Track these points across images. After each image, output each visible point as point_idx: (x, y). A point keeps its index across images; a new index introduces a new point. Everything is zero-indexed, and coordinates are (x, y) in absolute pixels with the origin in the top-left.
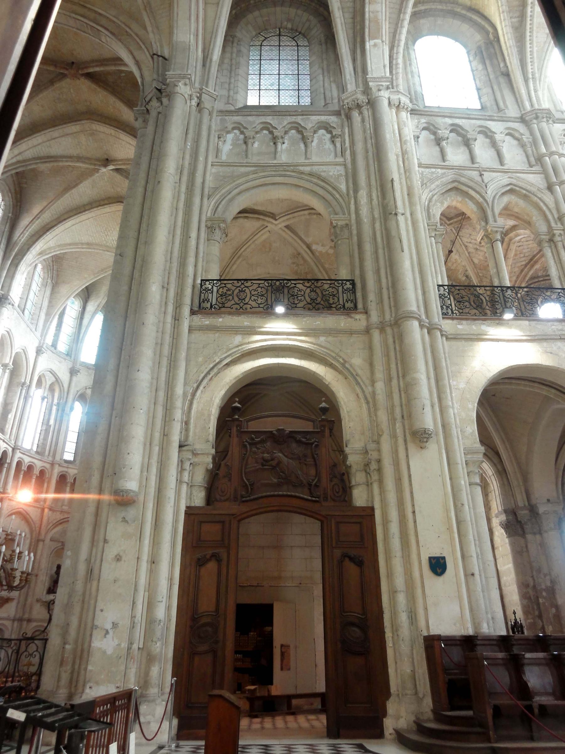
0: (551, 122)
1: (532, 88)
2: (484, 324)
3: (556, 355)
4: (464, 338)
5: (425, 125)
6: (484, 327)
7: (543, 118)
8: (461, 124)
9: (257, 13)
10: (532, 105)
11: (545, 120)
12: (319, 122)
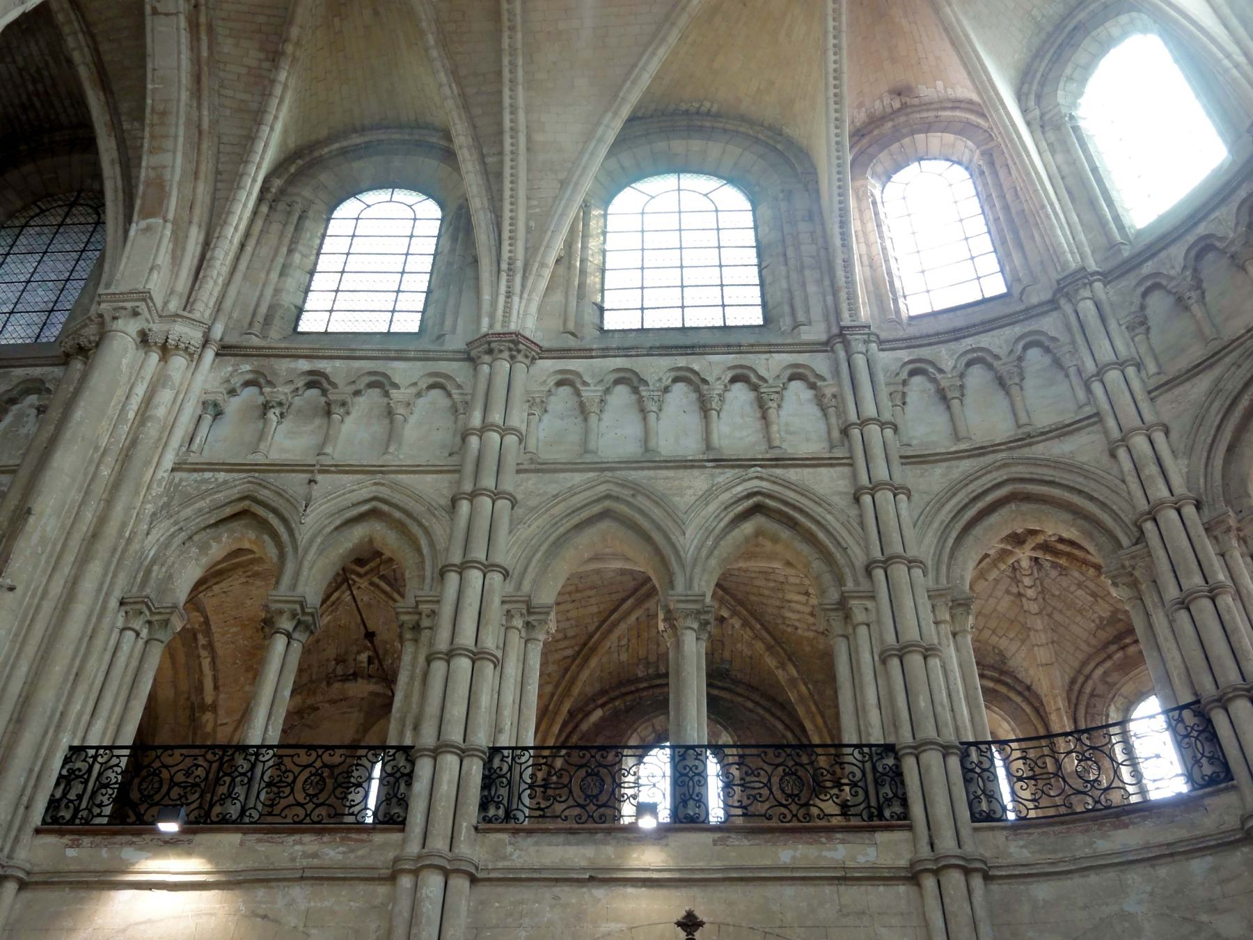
0: (520, 357)
1: (503, 288)
2: (133, 843)
3: (276, 921)
4: (71, 883)
5: (249, 377)
6: (127, 853)
7: (501, 351)
8: (328, 371)
9: (28, 168)
10: (491, 326)
11: (506, 354)
12: (23, 382)
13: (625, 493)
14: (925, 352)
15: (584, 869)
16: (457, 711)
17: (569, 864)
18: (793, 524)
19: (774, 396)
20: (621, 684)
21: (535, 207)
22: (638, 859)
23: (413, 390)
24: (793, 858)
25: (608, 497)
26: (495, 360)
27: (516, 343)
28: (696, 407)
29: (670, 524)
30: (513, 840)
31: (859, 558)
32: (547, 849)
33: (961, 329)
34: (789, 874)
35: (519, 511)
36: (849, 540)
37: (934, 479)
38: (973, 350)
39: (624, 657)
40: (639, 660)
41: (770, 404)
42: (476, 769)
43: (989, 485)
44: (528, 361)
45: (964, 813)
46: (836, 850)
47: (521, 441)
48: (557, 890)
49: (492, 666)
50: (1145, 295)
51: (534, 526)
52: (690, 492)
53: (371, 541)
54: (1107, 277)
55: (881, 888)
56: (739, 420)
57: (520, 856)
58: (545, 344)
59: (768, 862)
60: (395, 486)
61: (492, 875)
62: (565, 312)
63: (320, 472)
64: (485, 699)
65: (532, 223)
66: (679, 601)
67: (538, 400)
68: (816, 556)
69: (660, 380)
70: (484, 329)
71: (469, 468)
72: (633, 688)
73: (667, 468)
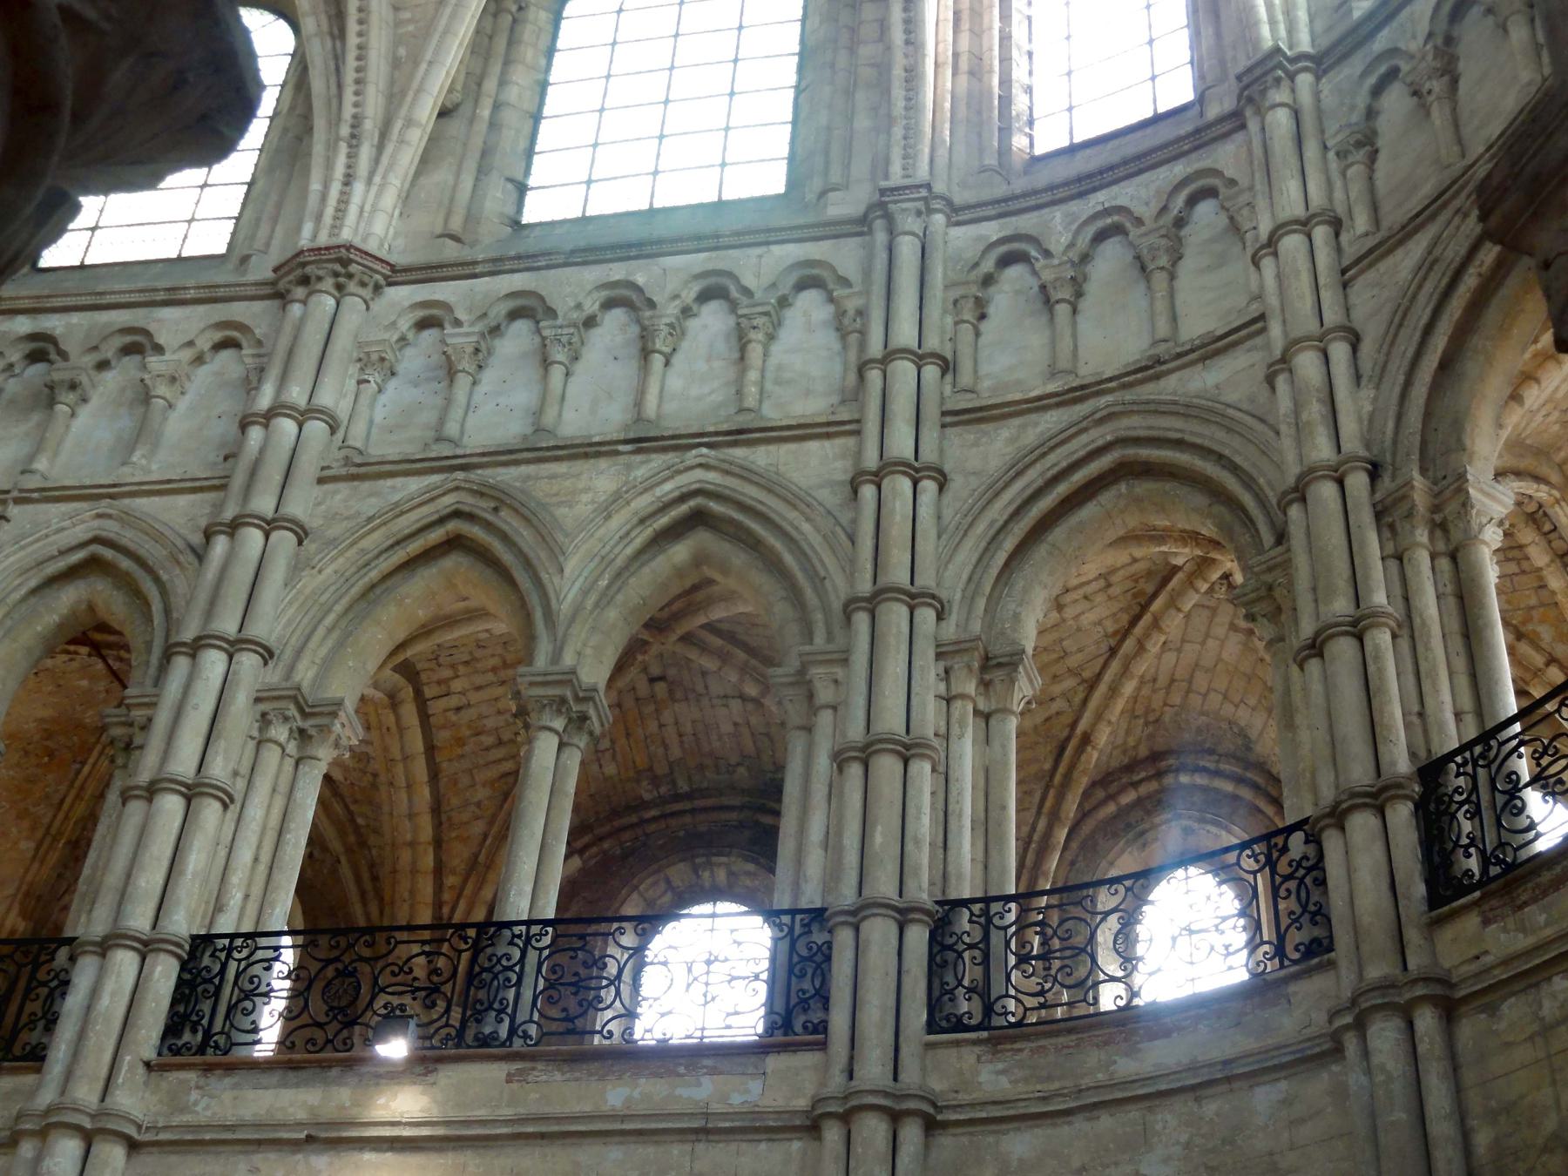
0: (352, 287)
7: (320, 279)
8: (57, 332)
10: (315, 236)
11: (328, 284)
13: (482, 507)
14: (1025, 223)
15: (300, 1125)
16: (150, 879)
17: (280, 1116)
18: (753, 544)
19: (759, 321)
20: (615, 813)
21: (409, 21)
22: (386, 1107)
23: (187, 354)
25: (457, 514)
26: (310, 294)
27: (345, 263)
28: (635, 350)
29: (543, 555)
30: (202, 1082)
32: (251, 1094)
33: (1090, 176)
34: (618, 1126)
35: (310, 546)
36: (830, 564)
37: (995, 448)
38: (1107, 212)
39: (610, 769)
40: (639, 772)
41: (753, 335)
42: (165, 974)
43: (1082, 453)
44: (367, 293)
45: (916, 1016)
46: (699, 1085)
48: (258, 1159)
49: (217, 805)
50: (1377, 91)
51: (329, 570)
52: (585, 498)
53: (91, 608)
54: (1321, 63)
55: (763, 1146)
56: (702, 366)
57: (207, 1108)
58: (393, 259)
59: (587, 1107)
60: (126, 519)
61: (163, 1136)
62: (452, 200)
63: (17, 501)
64: (195, 860)
65: (402, 51)
66: (532, 684)
67: (375, 357)
68: (783, 593)
69: (579, 306)
70: (305, 241)
71: (238, 481)
72: (634, 819)
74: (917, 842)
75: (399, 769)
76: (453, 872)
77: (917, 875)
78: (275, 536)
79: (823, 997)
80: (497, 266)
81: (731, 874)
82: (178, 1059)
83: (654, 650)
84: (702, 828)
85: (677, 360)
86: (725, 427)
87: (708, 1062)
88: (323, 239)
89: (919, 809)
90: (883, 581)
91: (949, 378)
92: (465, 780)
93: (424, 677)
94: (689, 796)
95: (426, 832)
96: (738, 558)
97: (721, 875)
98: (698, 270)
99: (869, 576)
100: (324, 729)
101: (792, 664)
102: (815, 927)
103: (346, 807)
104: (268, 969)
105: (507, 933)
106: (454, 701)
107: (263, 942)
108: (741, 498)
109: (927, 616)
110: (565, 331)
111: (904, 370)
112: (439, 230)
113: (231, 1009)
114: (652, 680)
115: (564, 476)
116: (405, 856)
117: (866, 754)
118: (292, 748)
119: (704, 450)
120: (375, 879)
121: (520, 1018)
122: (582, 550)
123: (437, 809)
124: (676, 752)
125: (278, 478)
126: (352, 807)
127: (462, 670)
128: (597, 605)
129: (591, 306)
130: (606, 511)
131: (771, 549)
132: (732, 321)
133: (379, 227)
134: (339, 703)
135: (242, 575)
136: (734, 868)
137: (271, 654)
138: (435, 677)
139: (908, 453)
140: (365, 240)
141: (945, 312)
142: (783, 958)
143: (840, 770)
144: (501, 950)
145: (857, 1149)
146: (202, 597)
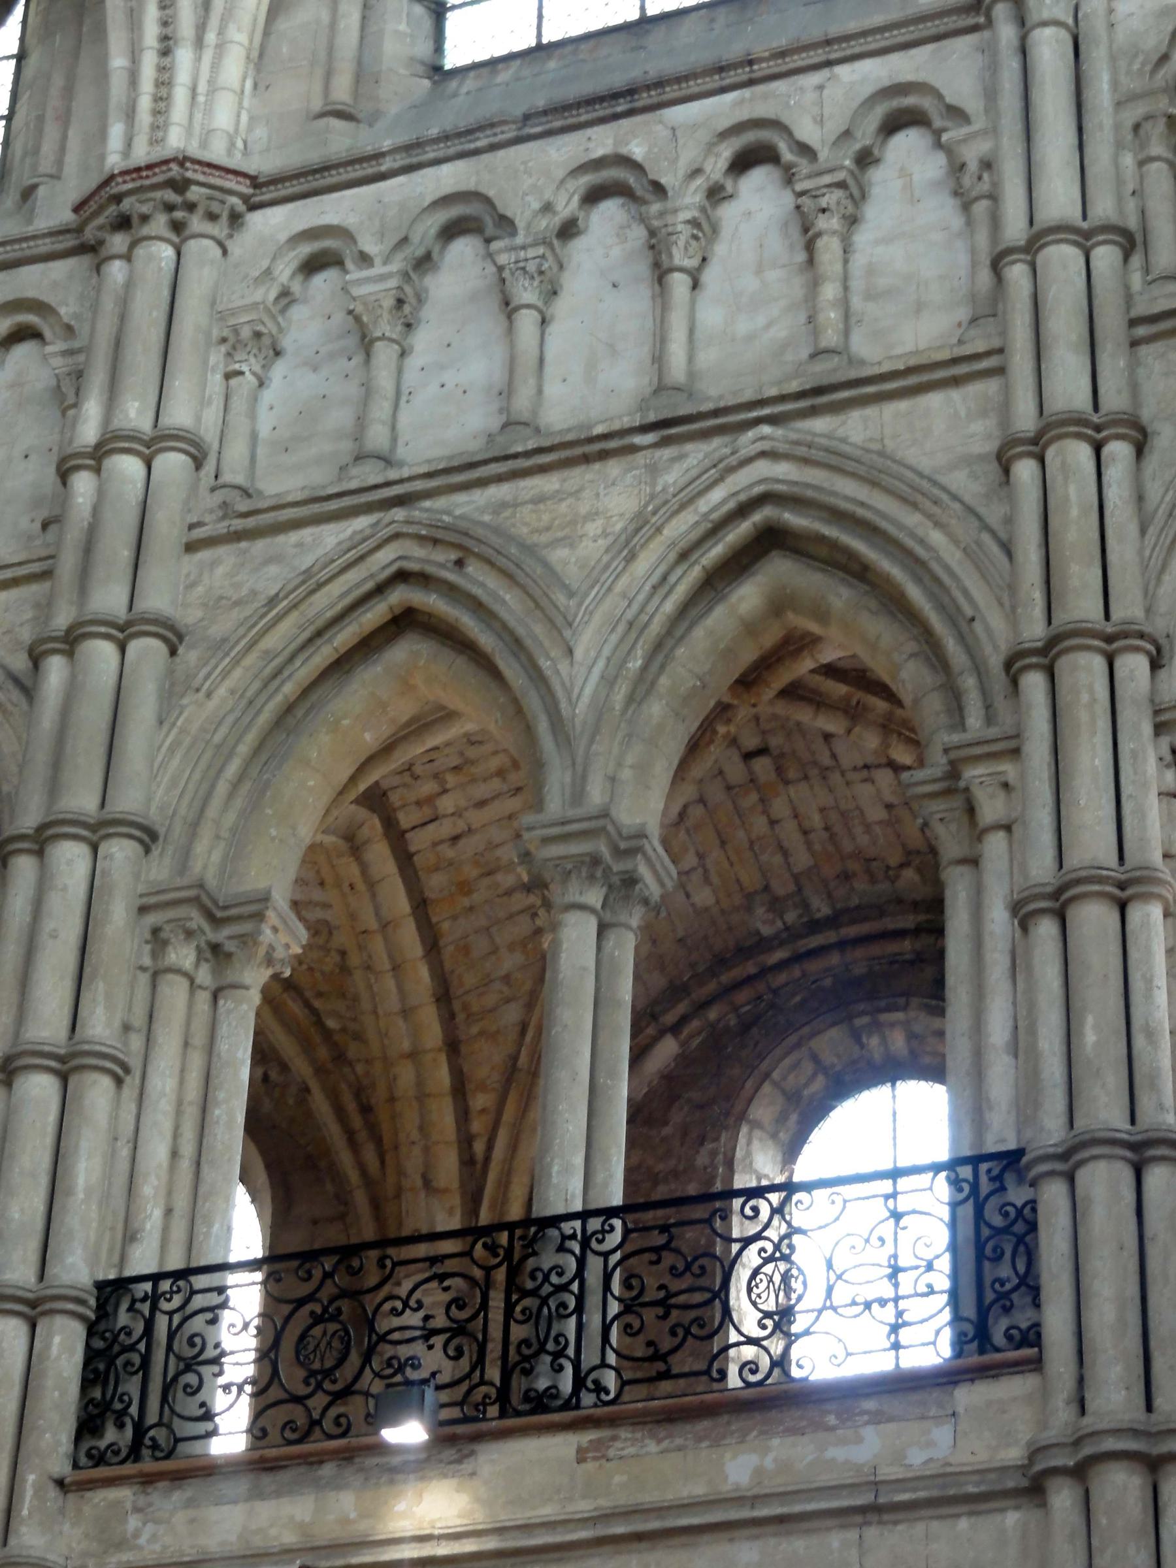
0: (196, 223)
7: (145, 218)
11: (159, 224)
13: (438, 560)
18: (857, 571)
19: (831, 198)
20: (721, 962)
24: (759, 1472)
25: (402, 576)
26: (133, 245)
27: (180, 186)
28: (643, 268)
29: (539, 629)
30: (142, 1501)
31: (1004, 644)
34: (745, 1513)
35: (189, 656)
39: (703, 897)
40: (749, 897)
41: (822, 223)
42: (65, 1345)
44: (219, 229)
46: (859, 1440)
47: (198, 463)
49: (106, 1082)
51: (222, 691)
52: (593, 528)
55: (963, 1524)
56: (750, 283)
57: (154, 1538)
58: (256, 165)
59: (699, 1490)
62: (331, 49)
64: (86, 1170)
66: (546, 841)
67: (246, 333)
68: (911, 647)
69: (547, 208)
70: (114, 161)
71: (68, 564)
72: (751, 968)
73: (543, 469)
74: (1151, 1034)
75: (378, 945)
76: (482, 1087)
77: (1154, 1086)
78: (134, 646)
79: (1030, 1286)
80: (414, 156)
81: (911, 1036)
82: (103, 1472)
83: (743, 713)
84: (859, 970)
85: (709, 276)
86: (794, 386)
87: (870, 1405)
88: (142, 153)
89: (1149, 981)
90: (1062, 618)
91: (1136, 260)
92: (480, 945)
93: (395, 798)
94: (833, 922)
95: (433, 1034)
96: (840, 595)
97: (898, 1042)
98: (725, 123)
99: (1038, 611)
100: (247, 940)
101: (938, 763)
102: (1010, 1179)
103: (307, 1005)
104: (214, 1321)
105: (553, 1233)
106: (445, 829)
107: (200, 1281)
108: (832, 500)
109: (1134, 666)
110: (531, 253)
111: (1062, 258)
112: (317, 105)
113: (167, 1388)
114: (748, 756)
115: (558, 496)
116: (406, 1075)
117: (1059, 903)
118: (204, 976)
119: (766, 429)
120: (366, 1110)
121: (590, 1358)
122: (597, 618)
123: (444, 996)
124: (802, 860)
125: (125, 554)
126: (317, 1004)
127: (451, 780)
128: (630, 699)
129: (567, 205)
130: (627, 548)
131: (887, 579)
132: (787, 199)
133: (223, 118)
134: (265, 899)
135: (93, 716)
136: (917, 1028)
137: (153, 835)
138: (412, 796)
139: (1081, 400)
140: (204, 144)
141: (1119, 145)
142: (967, 1229)
143: (1024, 927)
144: (548, 1259)
145: (1101, 1520)
146: (41, 757)
